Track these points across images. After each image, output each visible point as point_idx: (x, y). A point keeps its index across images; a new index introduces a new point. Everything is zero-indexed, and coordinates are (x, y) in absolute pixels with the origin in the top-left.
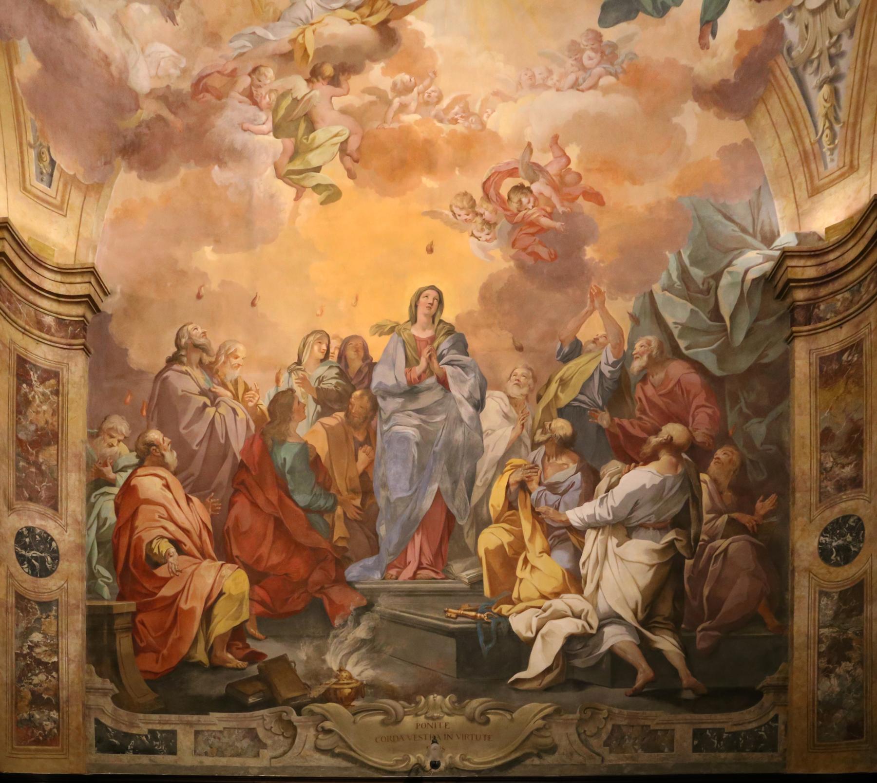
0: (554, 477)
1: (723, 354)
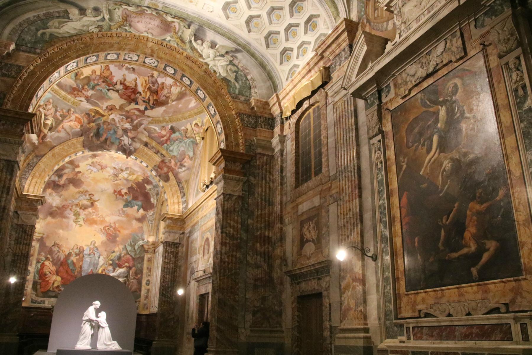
0: (109, 269)
1: (135, 255)
